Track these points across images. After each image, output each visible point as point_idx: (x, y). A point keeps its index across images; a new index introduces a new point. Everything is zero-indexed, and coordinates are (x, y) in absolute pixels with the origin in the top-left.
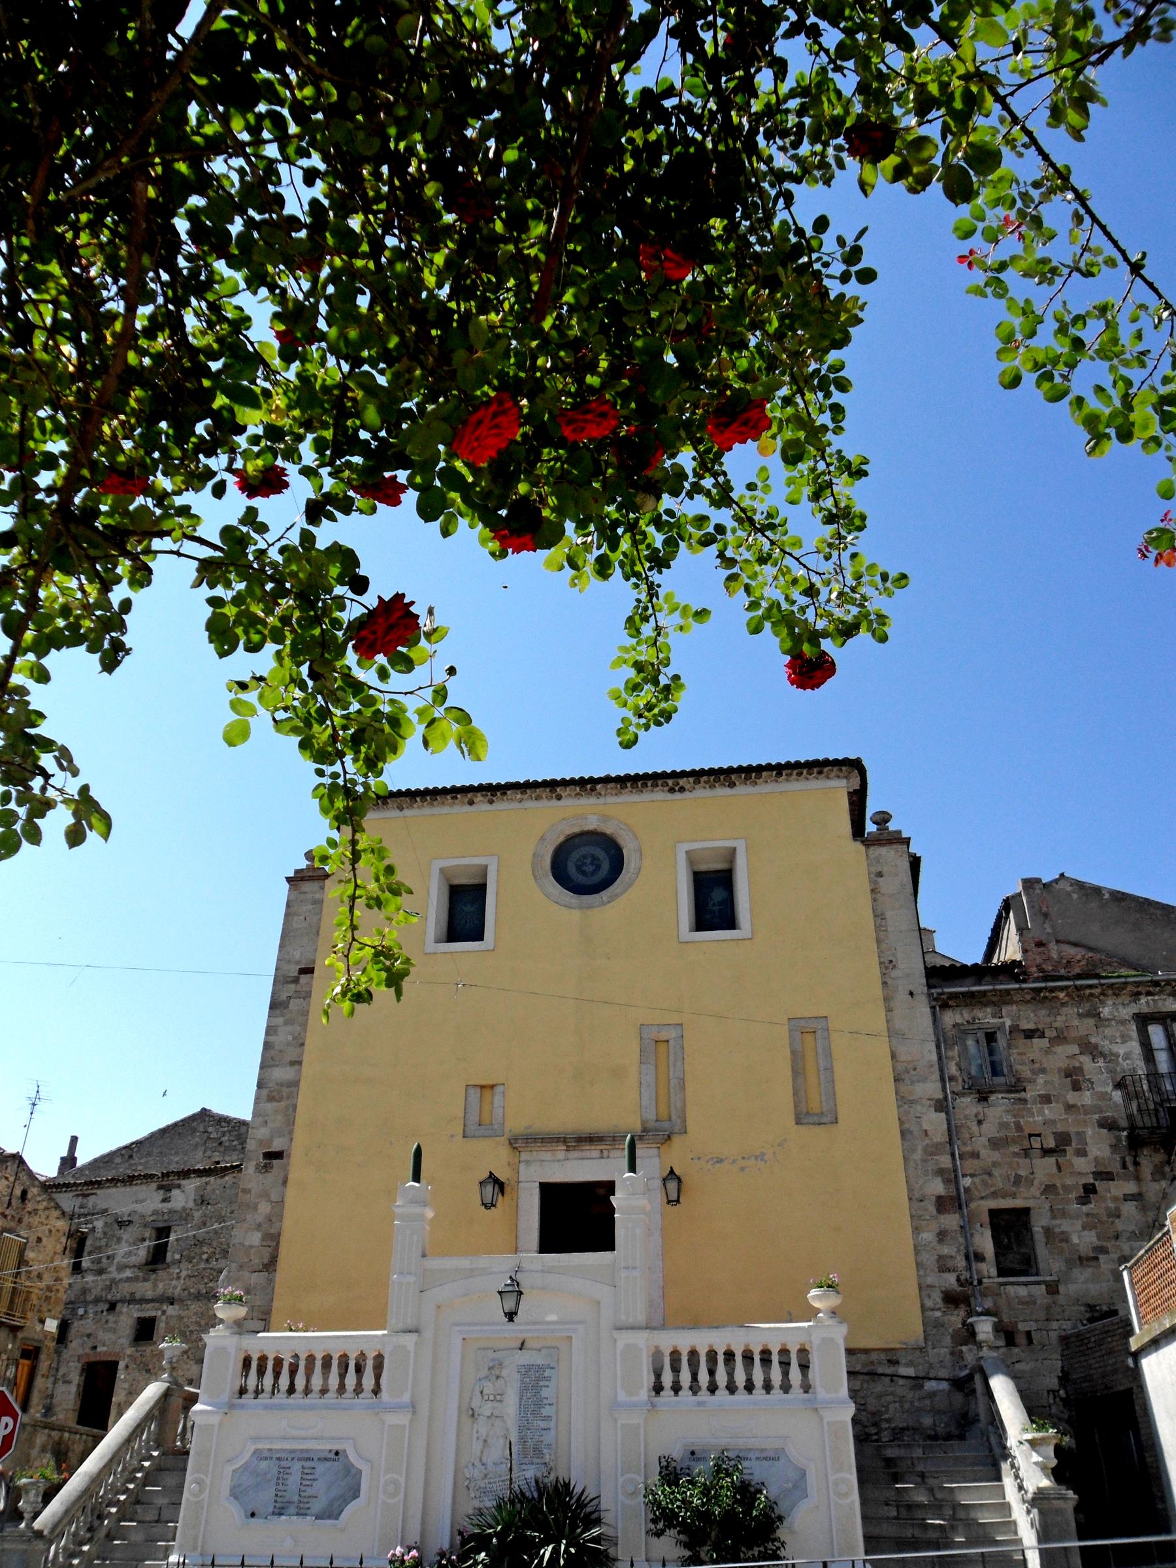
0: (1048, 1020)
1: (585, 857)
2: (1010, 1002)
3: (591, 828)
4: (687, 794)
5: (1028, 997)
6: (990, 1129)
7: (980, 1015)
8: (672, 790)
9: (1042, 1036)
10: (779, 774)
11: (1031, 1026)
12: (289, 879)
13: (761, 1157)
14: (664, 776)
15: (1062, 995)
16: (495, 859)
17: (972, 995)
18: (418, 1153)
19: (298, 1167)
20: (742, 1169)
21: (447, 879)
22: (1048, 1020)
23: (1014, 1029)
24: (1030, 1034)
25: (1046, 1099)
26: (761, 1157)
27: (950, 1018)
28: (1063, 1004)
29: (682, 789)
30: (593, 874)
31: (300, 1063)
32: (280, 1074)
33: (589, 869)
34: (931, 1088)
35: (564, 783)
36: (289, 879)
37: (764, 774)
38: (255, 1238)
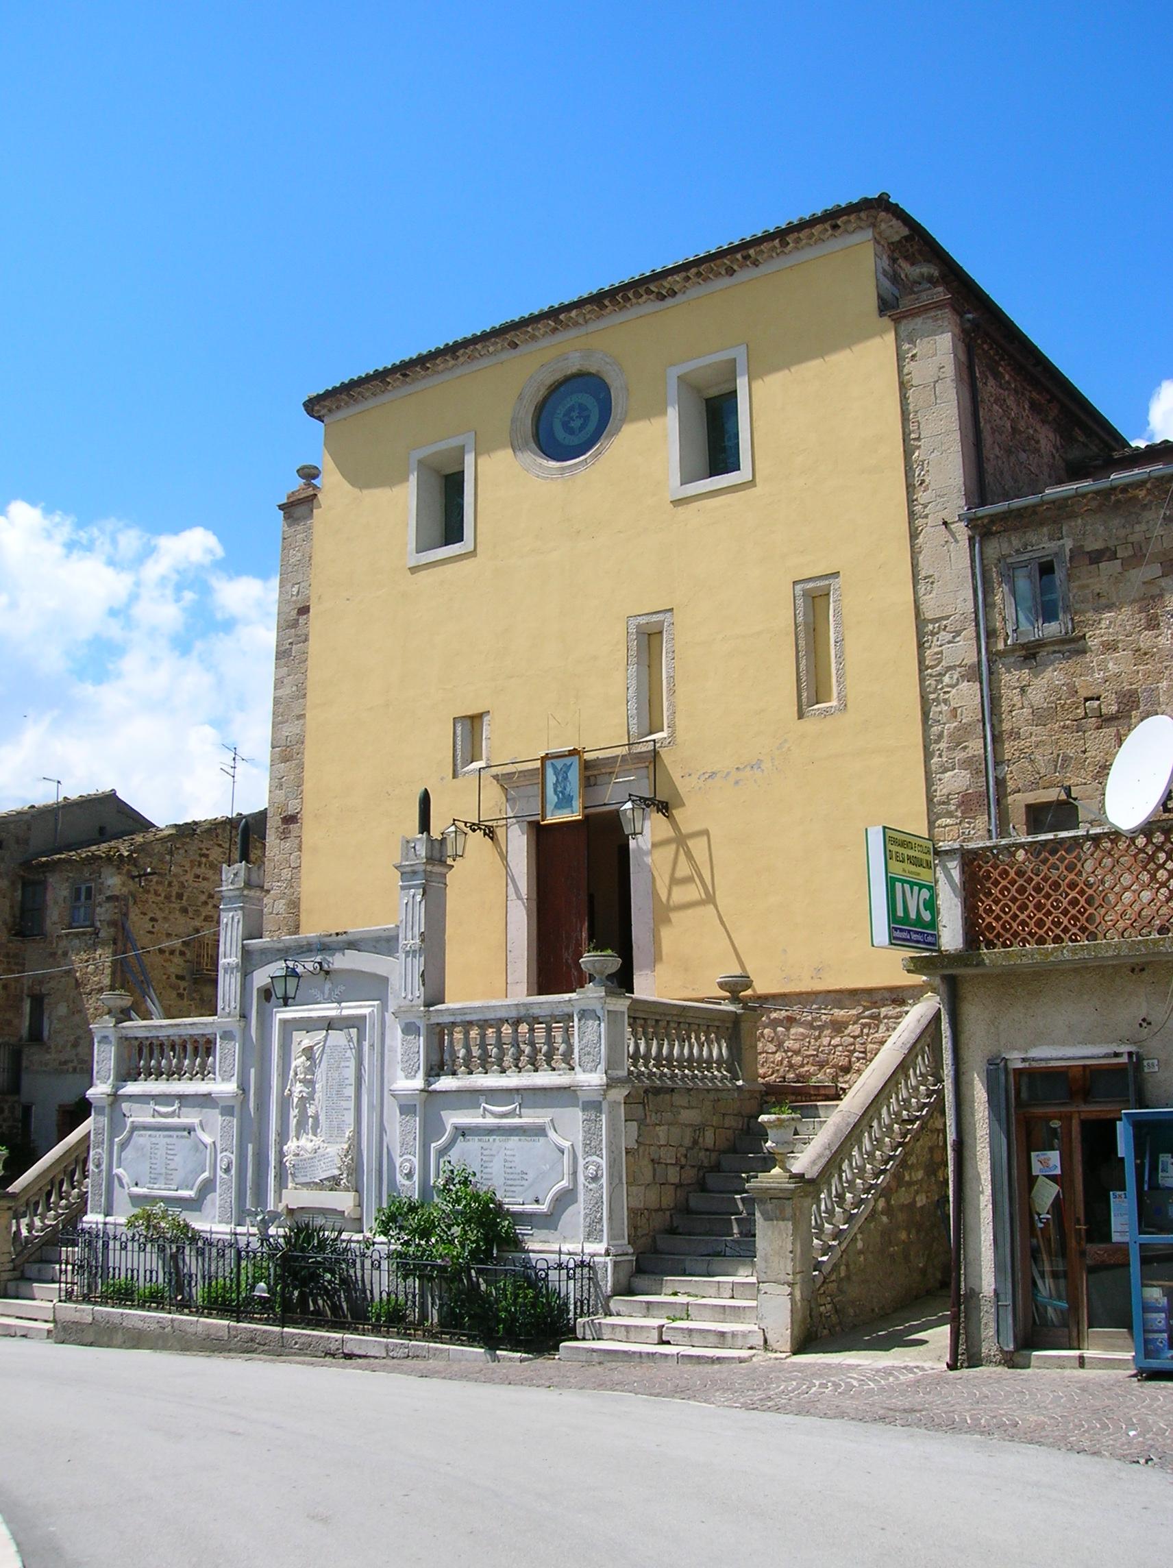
0: (1122, 533)
1: (572, 409)
2: (1072, 516)
3: (574, 370)
4: (680, 298)
5: (1094, 504)
6: (1037, 696)
7: (1034, 540)
8: (661, 297)
9: (1114, 556)
10: (784, 244)
11: (1098, 545)
12: (281, 507)
13: (756, 765)
14: (644, 281)
15: (1141, 494)
16: (743, 349)
17: (1019, 513)
18: (425, 801)
19: (310, 831)
20: (737, 783)
21: (437, 472)
22: (1122, 533)
23: (1076, 553)
24: (1096, 557)
25: (1111, 647)
26: (756, 765)
27: (995, 548)
28: (1145, 507)
29: (673, 293)
30: (582, 428)
31: (304, 715)
32: (288, 730)
33: (576, 424)
34: (964, 650)
35: (756, 242)
36: (281, 507)
37: (790, 239)
38: (281, 906)
